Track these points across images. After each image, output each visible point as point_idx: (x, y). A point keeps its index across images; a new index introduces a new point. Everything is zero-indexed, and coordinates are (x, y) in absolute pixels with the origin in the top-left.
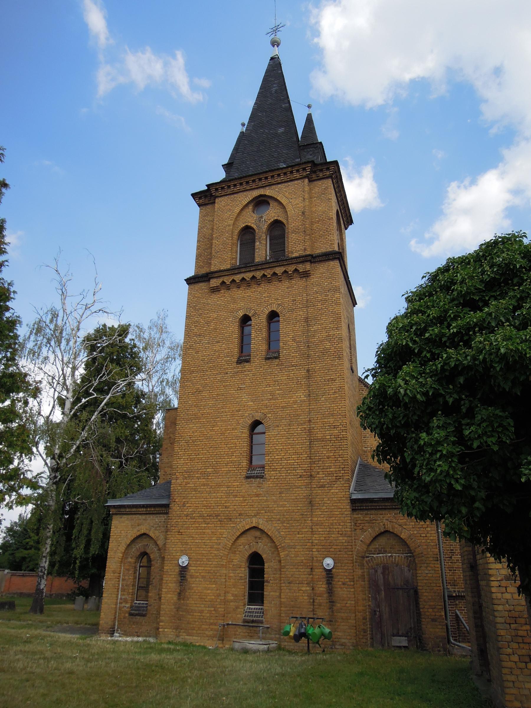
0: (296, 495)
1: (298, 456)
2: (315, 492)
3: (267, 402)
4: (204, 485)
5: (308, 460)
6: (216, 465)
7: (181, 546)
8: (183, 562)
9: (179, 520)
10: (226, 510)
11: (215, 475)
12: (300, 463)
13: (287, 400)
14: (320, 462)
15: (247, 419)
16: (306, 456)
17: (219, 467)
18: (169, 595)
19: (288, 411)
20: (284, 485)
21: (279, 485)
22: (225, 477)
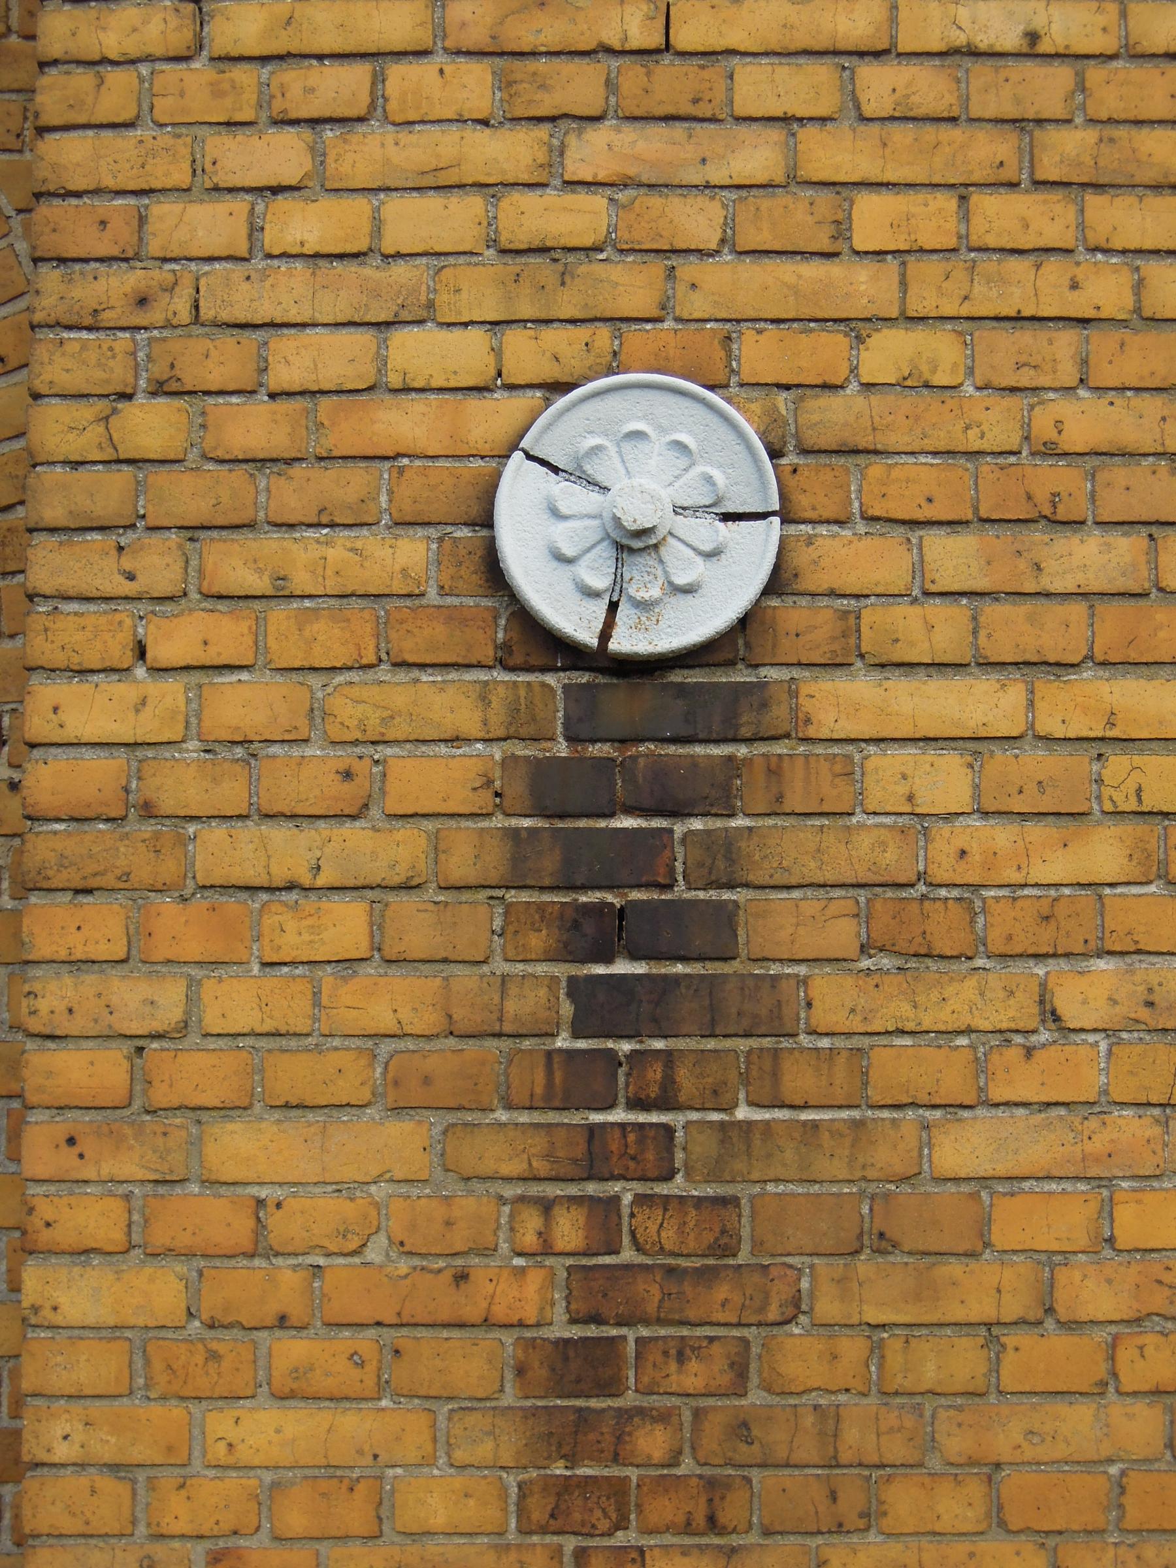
7: (512, 151)
8: (632, 544)
18: (264, 1432)
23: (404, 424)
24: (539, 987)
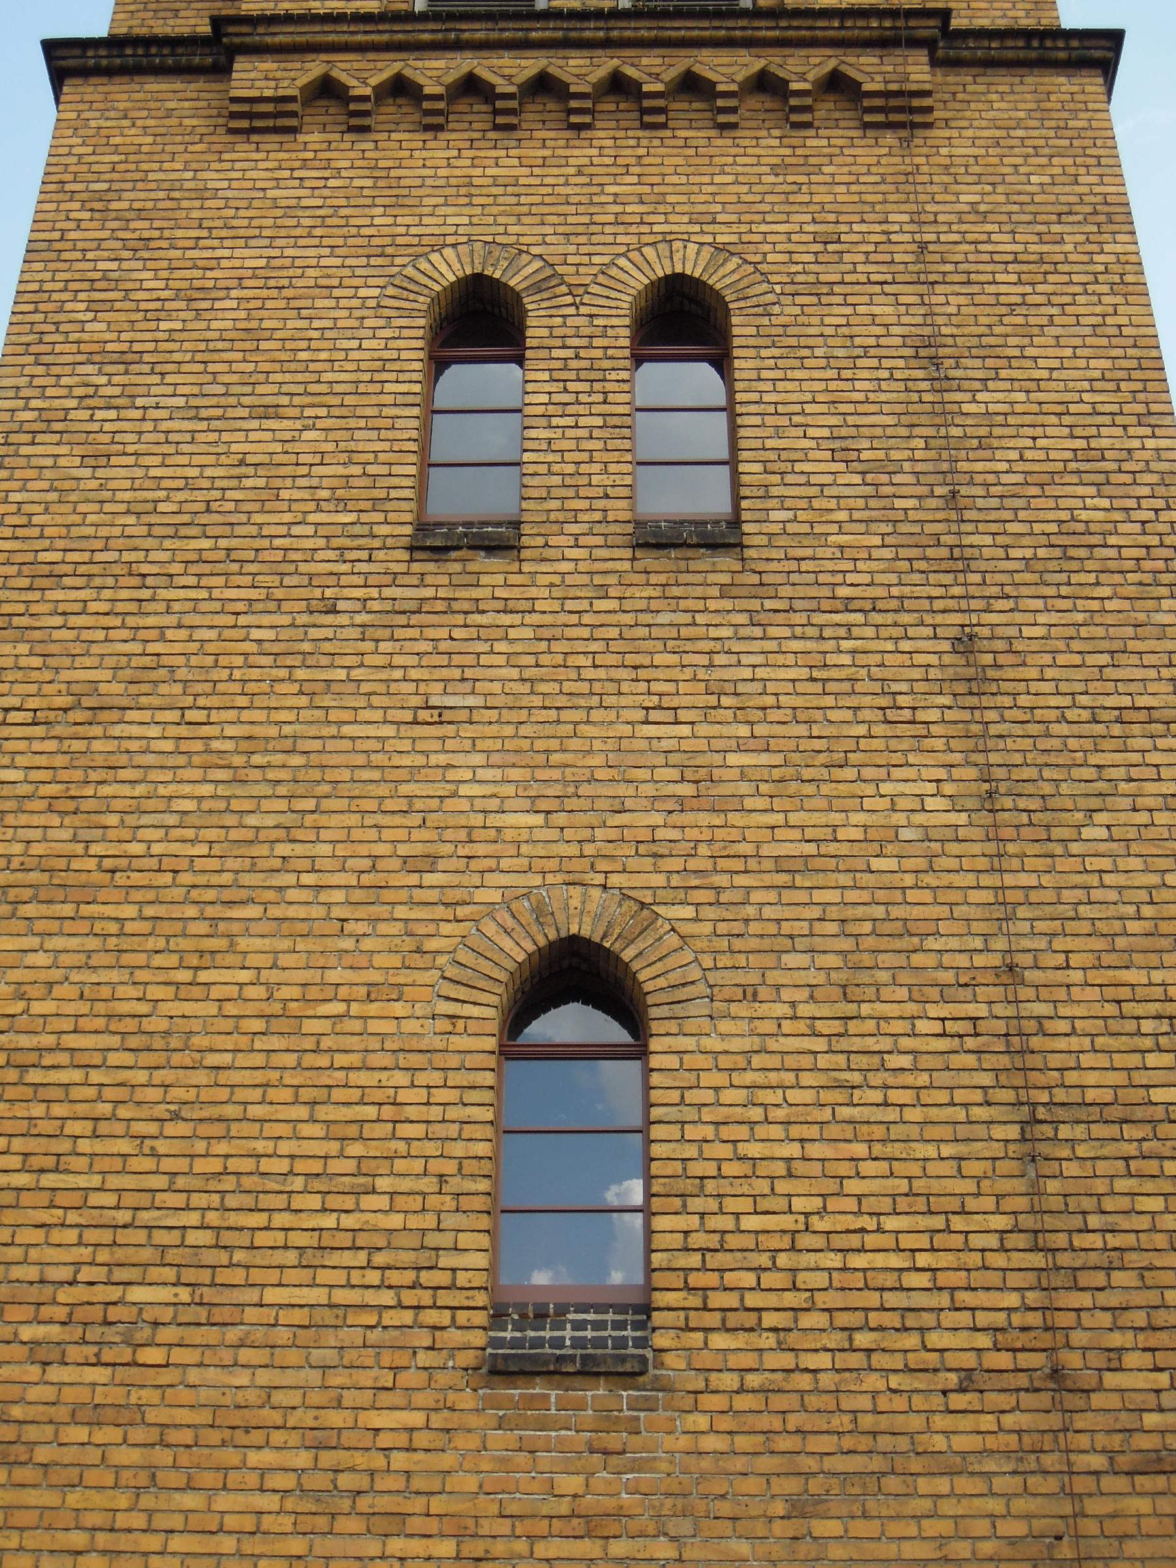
0: (944, 1527)
1: (938, 1222)
2: (1094, 1506)
3: (657, 819)
4: (94, 1415)
5: (1018, 1260)
6: (210, 1257)
11: (196, 1335)
12: (960, 1278)
13: (821, 819)
14: (1118, 1278)
15: (490, 928)
16: (1000, 1222)
17: (239, 1276)
19: (833, 896)
20: (826, 1443)
21: (784, 1443)
22: (293, 1357)
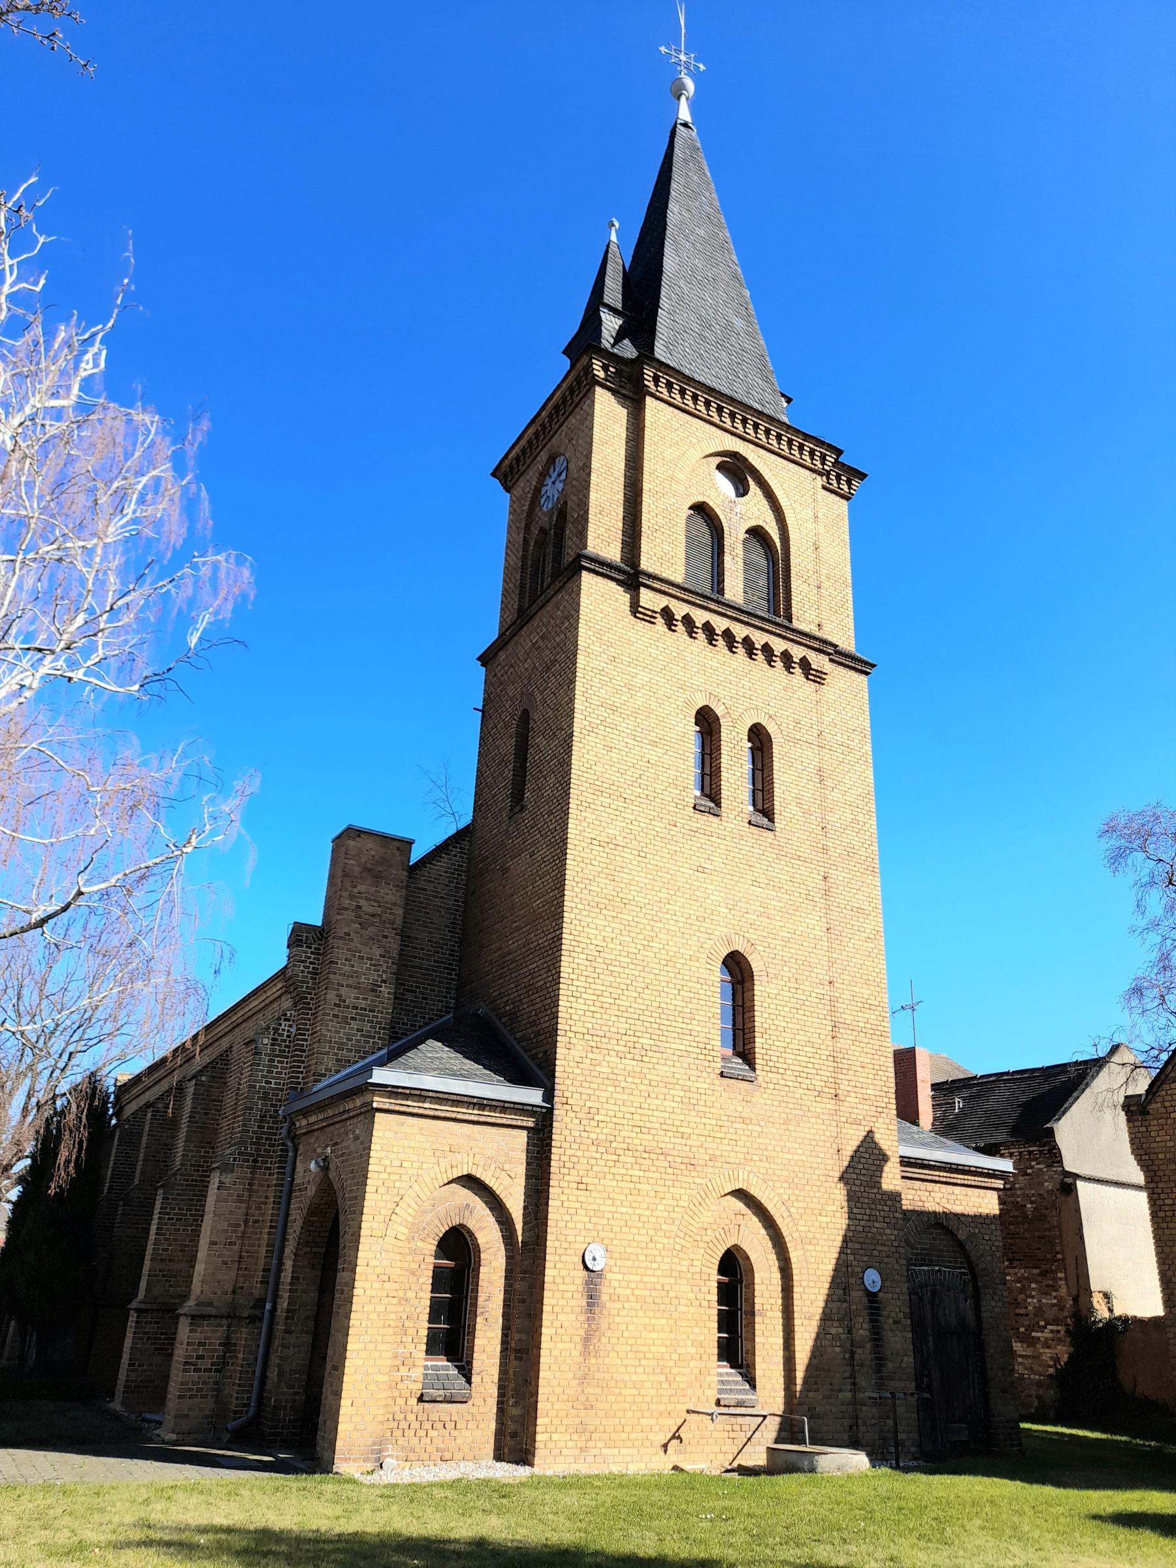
9: (580, 1153)
10: (683, 1142)
17: (664, 1039)
18: (560, 1345)
23: (577, 1246)
24: (584, 1303)
